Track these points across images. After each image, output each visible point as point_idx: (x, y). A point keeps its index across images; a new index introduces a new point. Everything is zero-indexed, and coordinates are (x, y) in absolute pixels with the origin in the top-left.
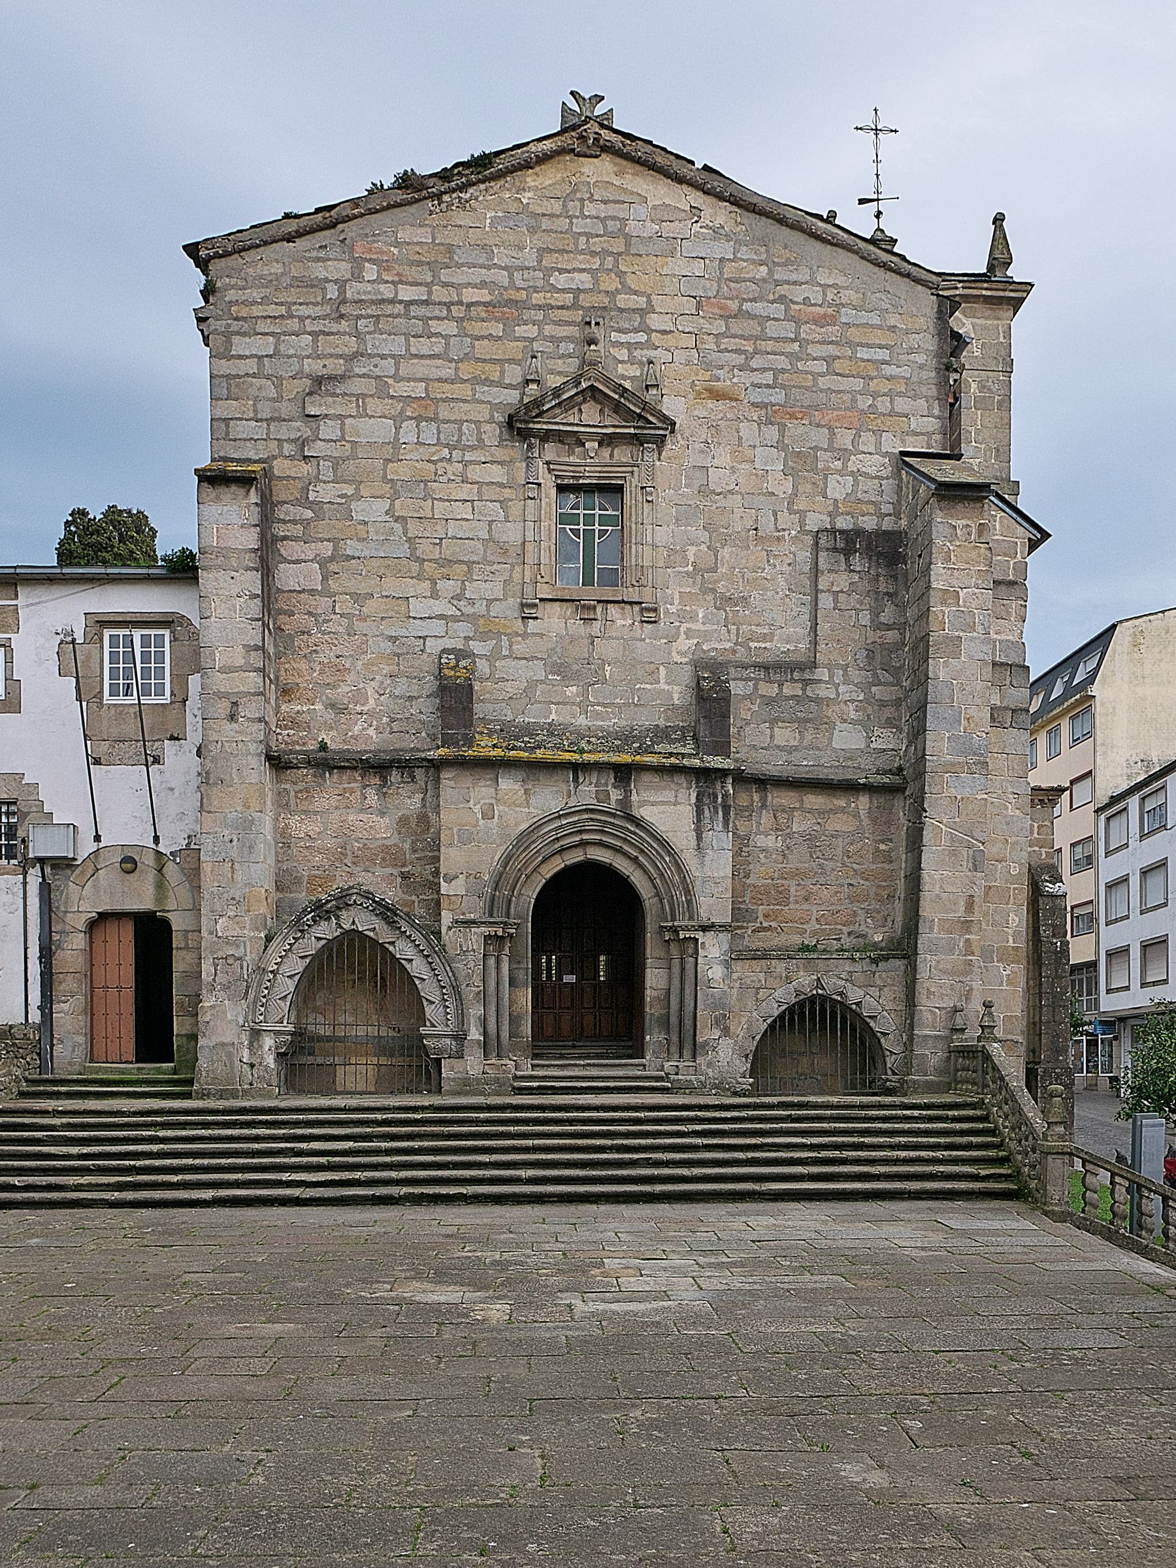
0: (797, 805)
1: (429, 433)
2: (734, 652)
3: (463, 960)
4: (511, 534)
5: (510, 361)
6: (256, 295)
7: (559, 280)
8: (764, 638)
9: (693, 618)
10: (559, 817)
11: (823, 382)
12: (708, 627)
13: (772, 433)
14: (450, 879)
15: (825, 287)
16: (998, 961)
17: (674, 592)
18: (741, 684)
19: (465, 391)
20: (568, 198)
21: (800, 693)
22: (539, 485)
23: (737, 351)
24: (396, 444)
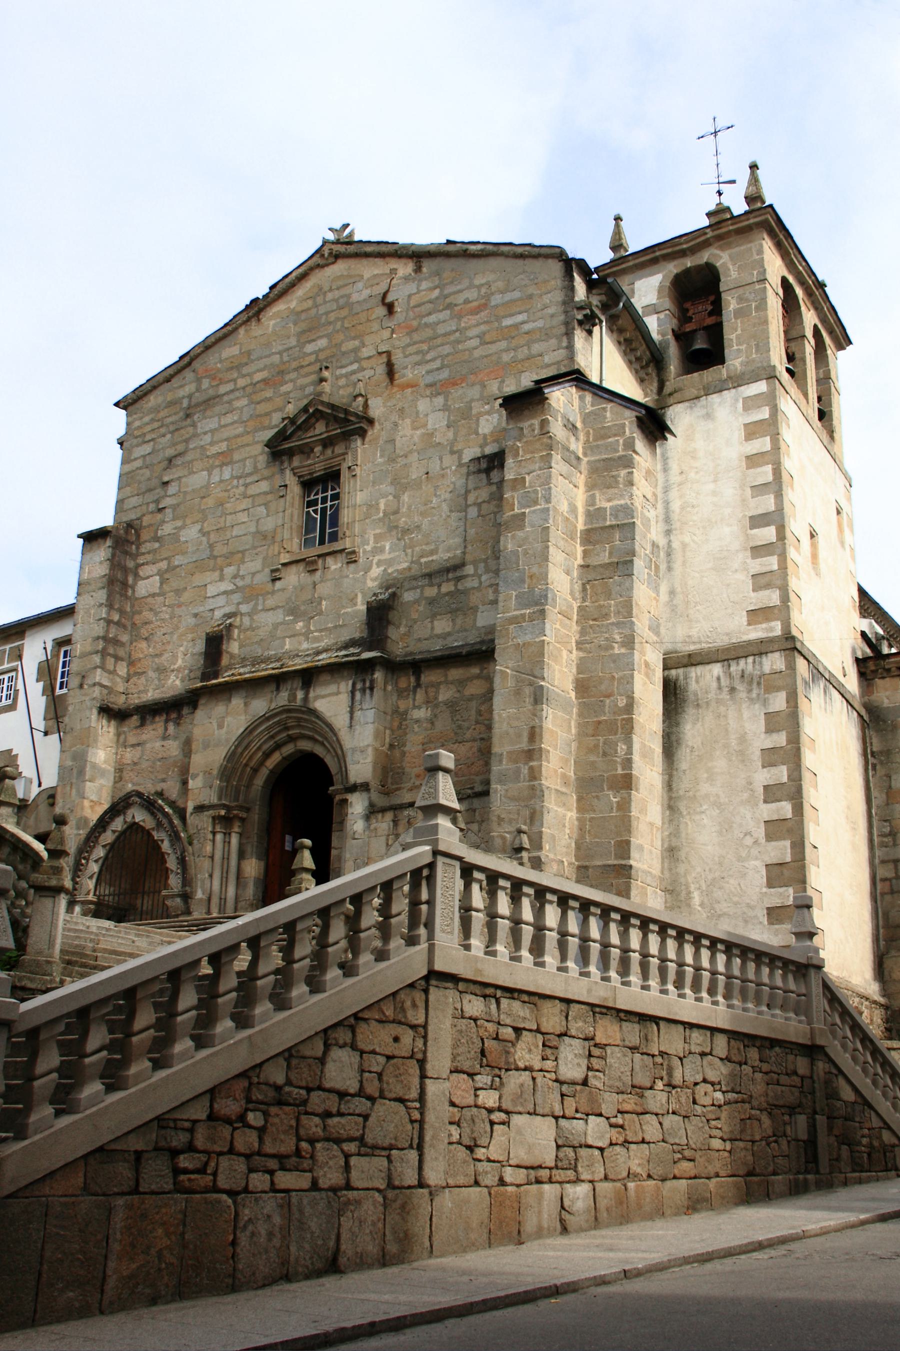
0: (443, 679)
1: (227, 473)
2: (409, 569)
4: (269, 524)
5: (275, 411)
6: (147, 419)
7: (309, 348)
8: (432, 553)
9: (382, 550)
10: (268, 719)
11: (477, 353)
12: (392, 555)
13: (440, 400)
14: (195, 777)
15: (479, 287)
16: (609, 789)
17: (370, 536)
18: (411, 593)
19: (248, 439)
20: (317, 295)
21: (453, 588)
22: (286, 486)
23: (417, 353)
24: (207, 486)
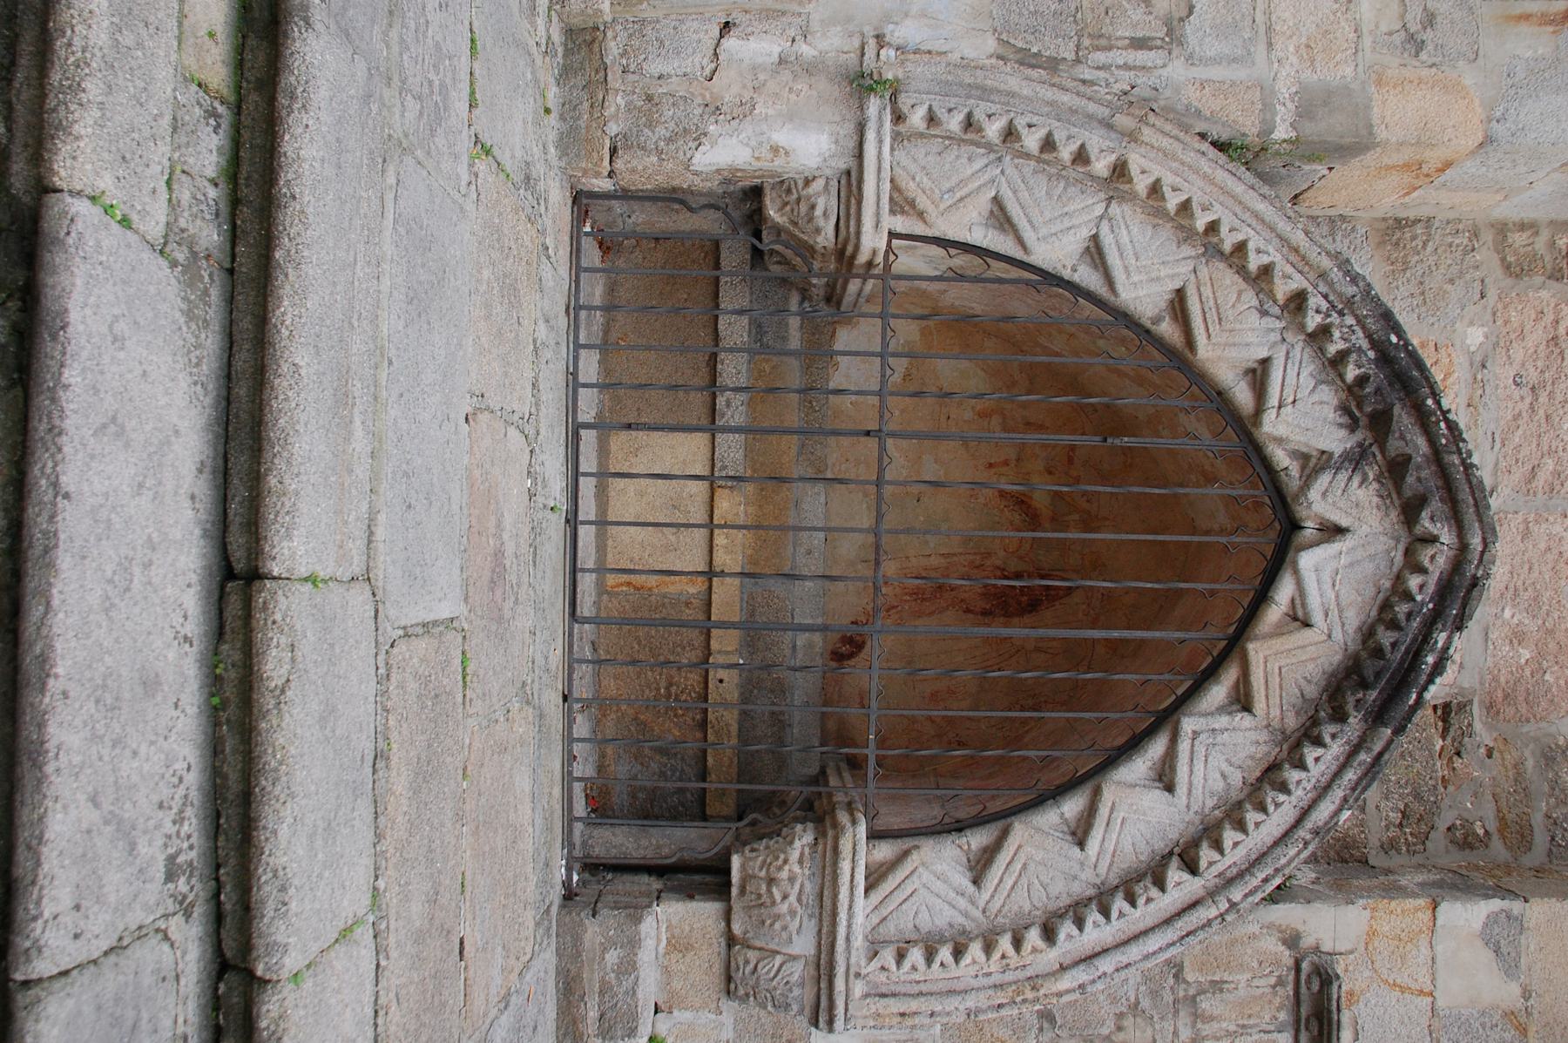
3: (1155, 994)
